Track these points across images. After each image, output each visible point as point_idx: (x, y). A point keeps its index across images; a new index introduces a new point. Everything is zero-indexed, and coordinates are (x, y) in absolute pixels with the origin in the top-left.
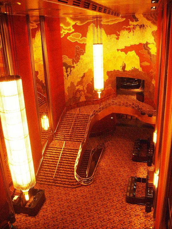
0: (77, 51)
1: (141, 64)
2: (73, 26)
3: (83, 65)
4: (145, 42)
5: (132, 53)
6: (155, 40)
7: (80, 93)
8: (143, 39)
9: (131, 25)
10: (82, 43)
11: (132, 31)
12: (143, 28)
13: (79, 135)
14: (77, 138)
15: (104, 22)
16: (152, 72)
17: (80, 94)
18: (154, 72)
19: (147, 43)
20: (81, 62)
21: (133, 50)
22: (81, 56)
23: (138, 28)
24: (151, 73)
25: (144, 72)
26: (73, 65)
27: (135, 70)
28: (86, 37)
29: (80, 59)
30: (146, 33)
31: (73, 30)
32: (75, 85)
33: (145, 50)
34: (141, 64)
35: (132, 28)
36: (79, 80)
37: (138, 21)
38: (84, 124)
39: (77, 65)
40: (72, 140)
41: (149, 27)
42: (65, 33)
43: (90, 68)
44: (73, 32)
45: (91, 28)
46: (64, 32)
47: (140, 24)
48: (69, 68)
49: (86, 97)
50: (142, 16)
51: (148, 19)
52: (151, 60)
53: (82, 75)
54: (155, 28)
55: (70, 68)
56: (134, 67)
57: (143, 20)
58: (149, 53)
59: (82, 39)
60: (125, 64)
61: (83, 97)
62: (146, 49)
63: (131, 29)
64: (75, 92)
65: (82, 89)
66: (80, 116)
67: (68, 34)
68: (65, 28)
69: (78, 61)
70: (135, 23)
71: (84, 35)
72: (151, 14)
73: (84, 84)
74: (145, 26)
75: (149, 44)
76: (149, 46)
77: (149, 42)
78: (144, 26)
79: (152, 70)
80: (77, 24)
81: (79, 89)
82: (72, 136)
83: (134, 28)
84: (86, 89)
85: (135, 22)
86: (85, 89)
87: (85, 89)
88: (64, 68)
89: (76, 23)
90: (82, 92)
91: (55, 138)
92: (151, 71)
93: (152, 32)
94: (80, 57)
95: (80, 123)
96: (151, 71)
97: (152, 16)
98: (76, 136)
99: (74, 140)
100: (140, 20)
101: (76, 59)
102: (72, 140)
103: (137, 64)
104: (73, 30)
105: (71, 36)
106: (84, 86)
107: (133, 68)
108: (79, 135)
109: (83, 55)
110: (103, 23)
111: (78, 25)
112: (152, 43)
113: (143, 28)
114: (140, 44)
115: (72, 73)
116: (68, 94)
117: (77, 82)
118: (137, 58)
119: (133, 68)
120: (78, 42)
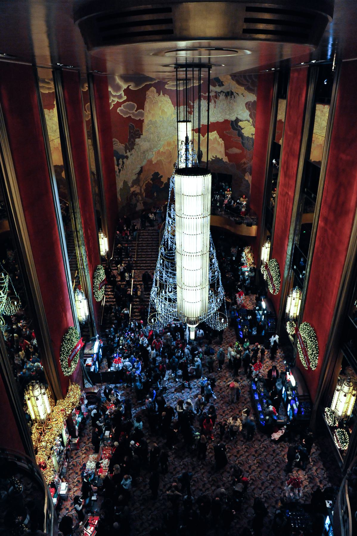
0: (131, 131)
1: (227, 151)
2: (125, 91)
3: (140, 154)
4: (234, 119)
5: (213, 135)
6: (250, 116)
7: (135, 197)
8: (230, 114)
9: (212, 91)
10: (138, 119)
11: (213, 101)
12: (231, 97)
13: (149, 260)
14: (146, 265)
15: (170, 86)
16: (244, 163)
18: (250, 162)
19: (237, 120)
20: (137, 150)
21: (214, 131)
22: (137, 140)
23: (222, 97)
24: (243, 165)
25: (231, 163)
26: (125, 155)
27: (217, 160)
28: (144, 110)
29: (135, 144)
30: (235, 104)
31: (125, 98)
32: (130, 185)
33: (234, 130)
34: (227, 151)
35: (213, 96)
36: (135, 177)
37: (223, 85)
38: (151, 243)
39: (131, 155)
40: (139, 268)
41: (240, 94)
42: (114, 103)
43: (149, 158)
44: (124, 102)
45: (152, 93)
46: (113, 101)
47: (226, 91)
48: (121, 159)
49: (145, 203)
50: (230, 77)
51: (239, 83)
52: (244, 146)
53: (138, 170)
54: (252, 98)
55: (123, 160)
56: (216, 156)
57: (231, 85)
58: (241, 135)
59: (138, 112)
60: (201, 151)
61: (140, 203)
62: (234, 129)
63: (212, 98)
66: (143, 233)
67: (119, 104)
68: (114, 94)
69: (133, 148)
70: (218, 89)
71: (141, 106)
72: (245, 77)
73: (141, 183)
74: (235, 94)
75: (241, 121)
76: (240, 124)
77: (240, 117)
78: (232, 93)
79: (244, 160)
80: (130, 87)
81: (135, 191)
82: (138, 262)
83: (216, 97)
84: (145, 192)
85: (217, 87)
86: (143, 191)
88: (115, 158)
89: (129, 86)
90: (140, 196)
91: (112, 267)
92: (243, 161)
93: (246, 104)
95: (145, 242)
96: (243, 161)
97: (246, 79)
98: (144, 262)
99: (142, 268)
100: (226, 84)
101: (131, 145)
102: (139, 268)
103: (221, 152)
104: (125, 98)
105: (122, 108)
106: (141, 187)
107: (213, 157)
108: (149, 260)
109: (139, 137)
110: (168, 87)
111: (132, 89)
112: (245, 121)
113: (231, 97)
114: (226, 121)
115: (125, 167)
116: (120, 200)
117: (132, 180)
118: (220, 142)
119: (213, 157)
120: (132, 117)
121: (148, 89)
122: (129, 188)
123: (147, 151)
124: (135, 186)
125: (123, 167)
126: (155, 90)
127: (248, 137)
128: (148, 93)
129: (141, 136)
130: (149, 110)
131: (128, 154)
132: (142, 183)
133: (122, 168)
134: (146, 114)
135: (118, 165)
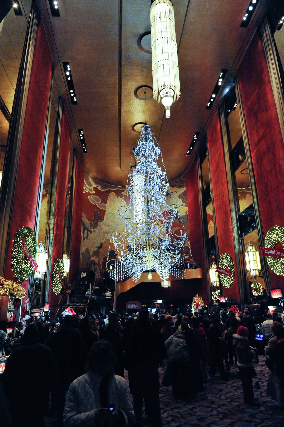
3: (101, 233)
7: (94, 266)
10: (101, 209)
20: (99, 229)
26: (91, 229)
53: (98, 244)
64: (89, 263)
65: (98, 263)
69: (96, 227)
71: (104, 201)
86: (101, 263)
87: (101, 263)
90: (98, 266)
106: (100, 259)
109: (102, 221)
115: (88, 237)
122: (90, 256)
123: (107, 232)
124: (95, 257)
125: (87, 237)
126: (115, 194)
128: (110, 195)
130: (110, 206)
131: (92, 230)
132: (101, 256)
133: (86, 237)
134: (107, 207)
135: (84, 233)
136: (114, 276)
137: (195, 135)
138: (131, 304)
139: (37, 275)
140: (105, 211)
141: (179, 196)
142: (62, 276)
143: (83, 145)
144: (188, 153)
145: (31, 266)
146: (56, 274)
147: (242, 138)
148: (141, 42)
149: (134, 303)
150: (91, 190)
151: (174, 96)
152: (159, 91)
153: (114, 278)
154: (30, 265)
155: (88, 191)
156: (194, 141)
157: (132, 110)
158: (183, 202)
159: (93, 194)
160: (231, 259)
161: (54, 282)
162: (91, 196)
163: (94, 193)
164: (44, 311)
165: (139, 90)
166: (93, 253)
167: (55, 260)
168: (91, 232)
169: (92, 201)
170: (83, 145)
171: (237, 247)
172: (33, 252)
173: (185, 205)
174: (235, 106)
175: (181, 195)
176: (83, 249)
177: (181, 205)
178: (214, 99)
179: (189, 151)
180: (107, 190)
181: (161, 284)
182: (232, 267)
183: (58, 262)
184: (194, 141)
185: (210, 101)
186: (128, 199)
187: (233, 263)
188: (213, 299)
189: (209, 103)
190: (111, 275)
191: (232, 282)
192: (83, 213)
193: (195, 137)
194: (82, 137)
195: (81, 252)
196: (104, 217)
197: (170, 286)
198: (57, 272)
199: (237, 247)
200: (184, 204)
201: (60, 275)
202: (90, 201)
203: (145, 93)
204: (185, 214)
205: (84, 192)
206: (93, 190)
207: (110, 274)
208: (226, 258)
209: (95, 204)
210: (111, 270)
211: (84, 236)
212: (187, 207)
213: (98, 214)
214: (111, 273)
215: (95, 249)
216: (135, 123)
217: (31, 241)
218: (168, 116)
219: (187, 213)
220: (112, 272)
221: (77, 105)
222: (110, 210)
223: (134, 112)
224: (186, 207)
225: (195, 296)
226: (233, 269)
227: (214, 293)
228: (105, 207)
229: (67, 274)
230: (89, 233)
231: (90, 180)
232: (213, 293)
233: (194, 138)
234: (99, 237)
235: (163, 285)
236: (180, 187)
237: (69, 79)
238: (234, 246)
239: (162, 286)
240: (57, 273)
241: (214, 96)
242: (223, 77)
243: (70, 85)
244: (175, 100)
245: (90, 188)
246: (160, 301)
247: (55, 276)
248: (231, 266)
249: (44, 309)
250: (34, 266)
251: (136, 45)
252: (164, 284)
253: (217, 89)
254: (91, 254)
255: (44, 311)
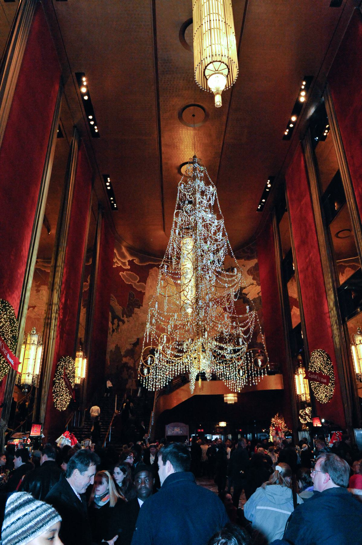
17: (128, 374)
20: (135, 319)
26: (123, 319)
39: (128, 321)
53: (134, 340)
69: (130, 316)
71: (144, 279)
90: (132, 372)
94: (134, 309)
109: (139, 308)
115: (119, 330)
121: (152, 268)
124: (128, 358)
125: (118, 329)
127: (254, 299)
129: (141, 307)
130: (151, 286)
131: (125, 319)
133: (116, 329)
134: (147, 288)
136: (149, 385)
137: (269, 181)
138: (174, 427)
139: (25, 379)
140: (144, 294)
141: (248, 271)
142: (72, 383)
143: (112, 199)
144: (259, 208)
145: (7, 363)
146: (59, 380)
147: (338, 172)
148: (185, 35)
149: (178, 426)
150: (124, 264)
151: (229, 76)
152: (204, 68)
153: (149, 387)
154: (4, 361)
155: (120, 264)
156: (267, 190)
157: (177, 143)
158: (254, 279)
159: (127, 270)
160: (329, 357)
161: (56, 391)
162: (125, 272)
163: (129, 267)
164: (30, 437)
165: (186, 110)
166: (125, 352)
167: (58, 358)
168: (124, 322)
169: (126, 279)
170: (112, 199)
171: (337, 340)
172: (10, 340)
173: (256, 284)
174: (325, 134)
175: (251, 270)
176: (111, 347)
177: (251, 284)
178: (294, 123)
179: (260, 206)
180: (148, 264)
181: (223, 398)
182: (330, 370)
183: (64, 360)
184: (267, 190)
185: (288, 127)
186: (176, 275)
187: (331, 364)
188: (302, 421)
189: (287, 130)
190: (145, 382)
191: (331, 395)
192: (112, 295)
193: (268, 183)
194: (108, 186)
195: (108, 350)
196: (142, 302)
197: (236, 401)
198: (61, 375)
199: (337, 340)
200: (255, 282)
201: (67, 380)
202: (123, 279)
203: (194, 116)
204: (257, 296)
205: (115, 266)
206: (127, 263)
207: (144, 381)
208: (319, 356)
209: (130, 283)
210: (145, 374)
211: (112, 327)
212: (260, 286)
213: (134, 298)
214: (146, 380)
215: (129, 347)
216: (182, 163)
217: (6, 322)
218: (218, 104)
219: (260, 294)
220: (147, 378)
221: (99, 138)
222: (151, 292)
223: (179, 147)
224: (257, 286)
225: (274, 418)
226: (332, 373)
227: (302, 412)
228: (144, 288)
229: (83, 380)
230: (121, 323)
231: (124, 250)
232: (300, 412)
233: (268, 184)
234: (135, 329)
235: (227, 400)
236: (249, 258)
237: (86, 98)
238: (332, 337)
239: (225, 402)
240: (62, 377)
241: (294, 119)
242: (307, 89)
243: (88, 107)
244: (231, 84)
245: (123, 261)
246: (223, 424)
247: (57, 383)
248: (329, 368)
249: (30, 433)
250: (13, 363)
251: (178, 41)
252: (228, 398)
253: (299, 109)
254: (122, 353)
255: (30, 437)
